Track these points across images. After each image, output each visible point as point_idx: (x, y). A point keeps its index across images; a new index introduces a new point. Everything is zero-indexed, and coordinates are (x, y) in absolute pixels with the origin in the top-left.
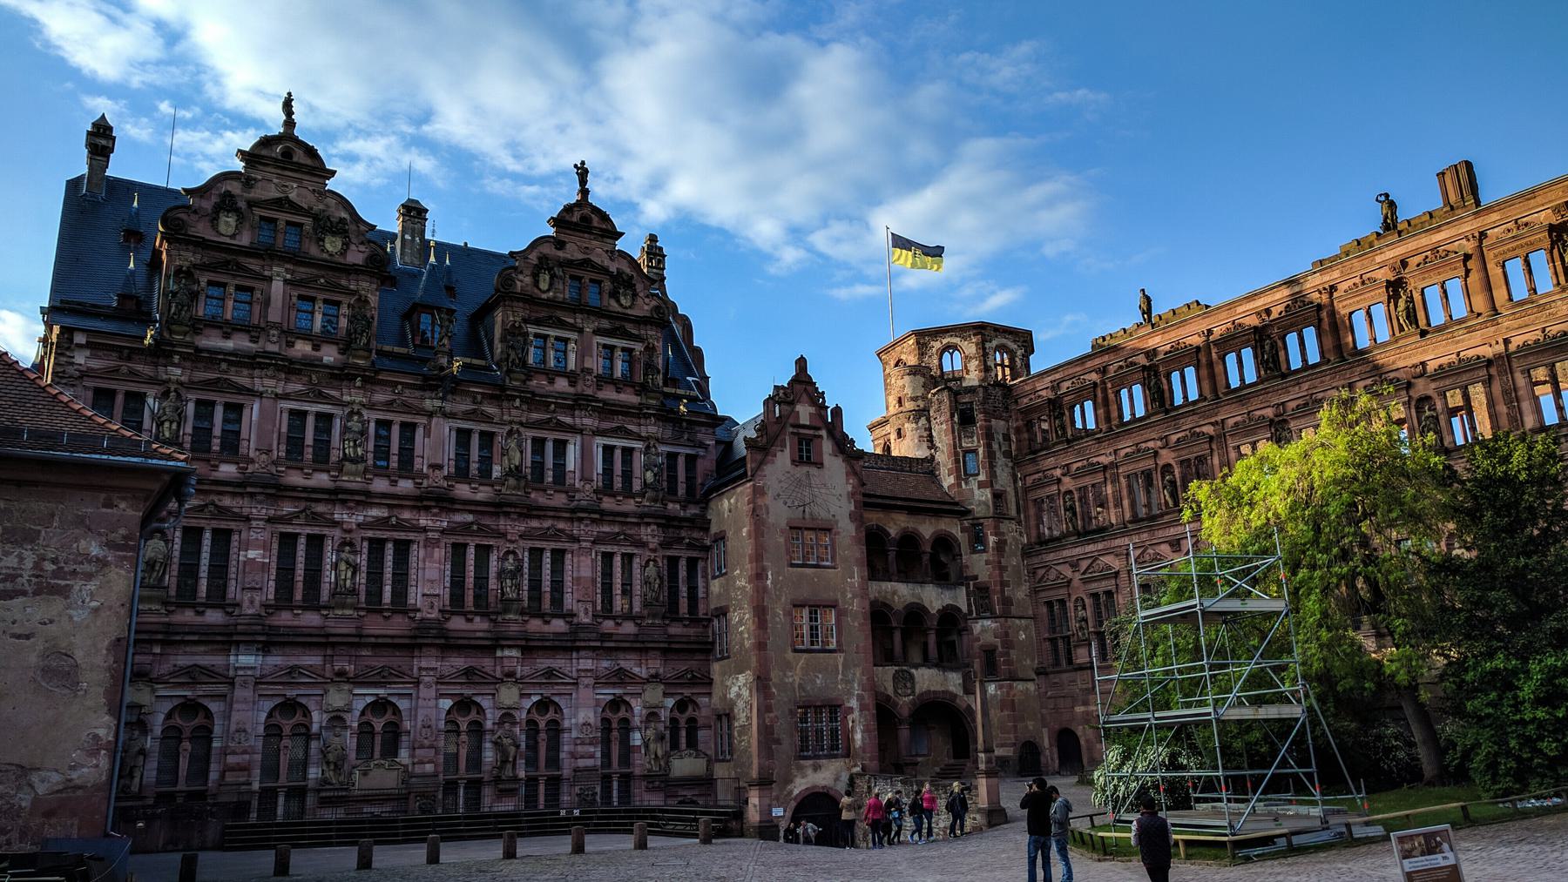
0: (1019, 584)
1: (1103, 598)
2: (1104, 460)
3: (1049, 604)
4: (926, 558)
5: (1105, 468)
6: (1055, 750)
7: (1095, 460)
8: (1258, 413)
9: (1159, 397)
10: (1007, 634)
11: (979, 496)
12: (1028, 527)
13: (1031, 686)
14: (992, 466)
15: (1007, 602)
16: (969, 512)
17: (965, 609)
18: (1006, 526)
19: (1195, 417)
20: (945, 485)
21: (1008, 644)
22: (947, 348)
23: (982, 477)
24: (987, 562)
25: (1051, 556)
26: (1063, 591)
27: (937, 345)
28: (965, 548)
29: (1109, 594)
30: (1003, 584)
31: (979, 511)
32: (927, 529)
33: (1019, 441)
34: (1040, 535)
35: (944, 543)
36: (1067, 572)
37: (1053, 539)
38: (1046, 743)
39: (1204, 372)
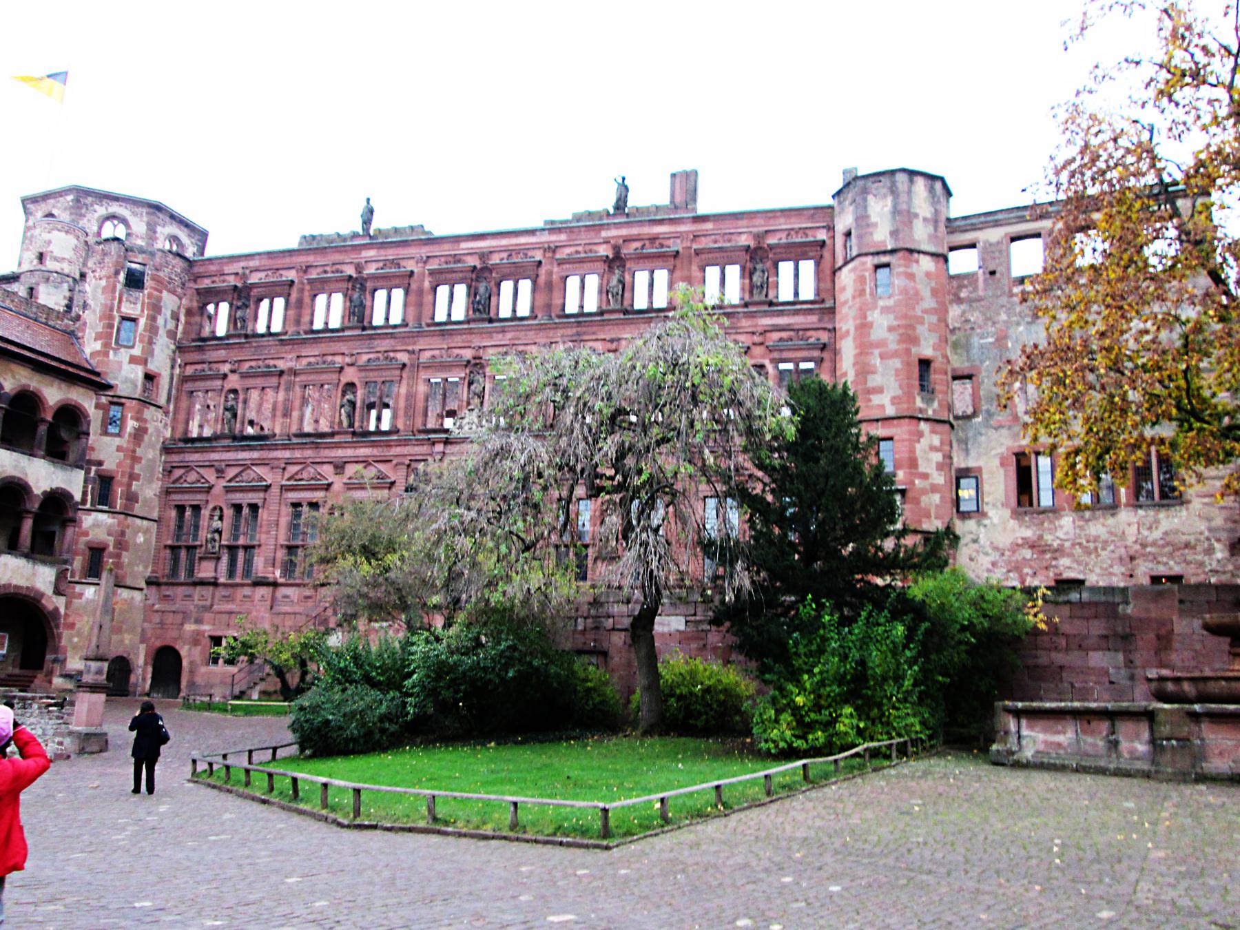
0: (150, 481)
1: (246, 511)
2: (281, 365)
3: (181, 509)
4: (43, 429)
5: (281, 373)
6: (150, 669)
7: (272, 362)
8: (456, 351)
9: (358, 313)
10: (123, 533)
11: (125, 375)
12: (174, 419)
13: (138, 596)
14: (151, 342)
15: (131, 498)
16: (109, 387)
17: (78, 497)
18: (149, 413)
19: (392, 342)
20: (88, 351)
21: (121, 544)
22: (112, 217)
23: (137, 351)
24: (119, 449)
25: (196, 457)
26: (199, 497)
27: (101, 210)
28: (95, 427)
29: (254, 508)
30: (133, 477)
31: (123, 389)
32: (53, 394)
33: (187, 323)
34: (186, 431)
35: (70, 416)
36: (211, 476)
37: (200, 439)
38: (141, 661)
39: (412, 298)
